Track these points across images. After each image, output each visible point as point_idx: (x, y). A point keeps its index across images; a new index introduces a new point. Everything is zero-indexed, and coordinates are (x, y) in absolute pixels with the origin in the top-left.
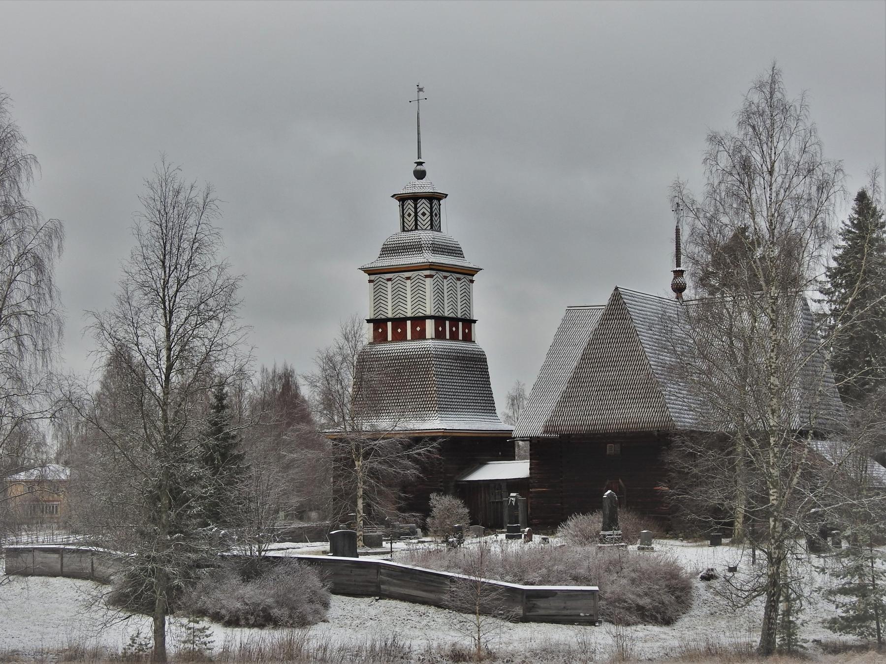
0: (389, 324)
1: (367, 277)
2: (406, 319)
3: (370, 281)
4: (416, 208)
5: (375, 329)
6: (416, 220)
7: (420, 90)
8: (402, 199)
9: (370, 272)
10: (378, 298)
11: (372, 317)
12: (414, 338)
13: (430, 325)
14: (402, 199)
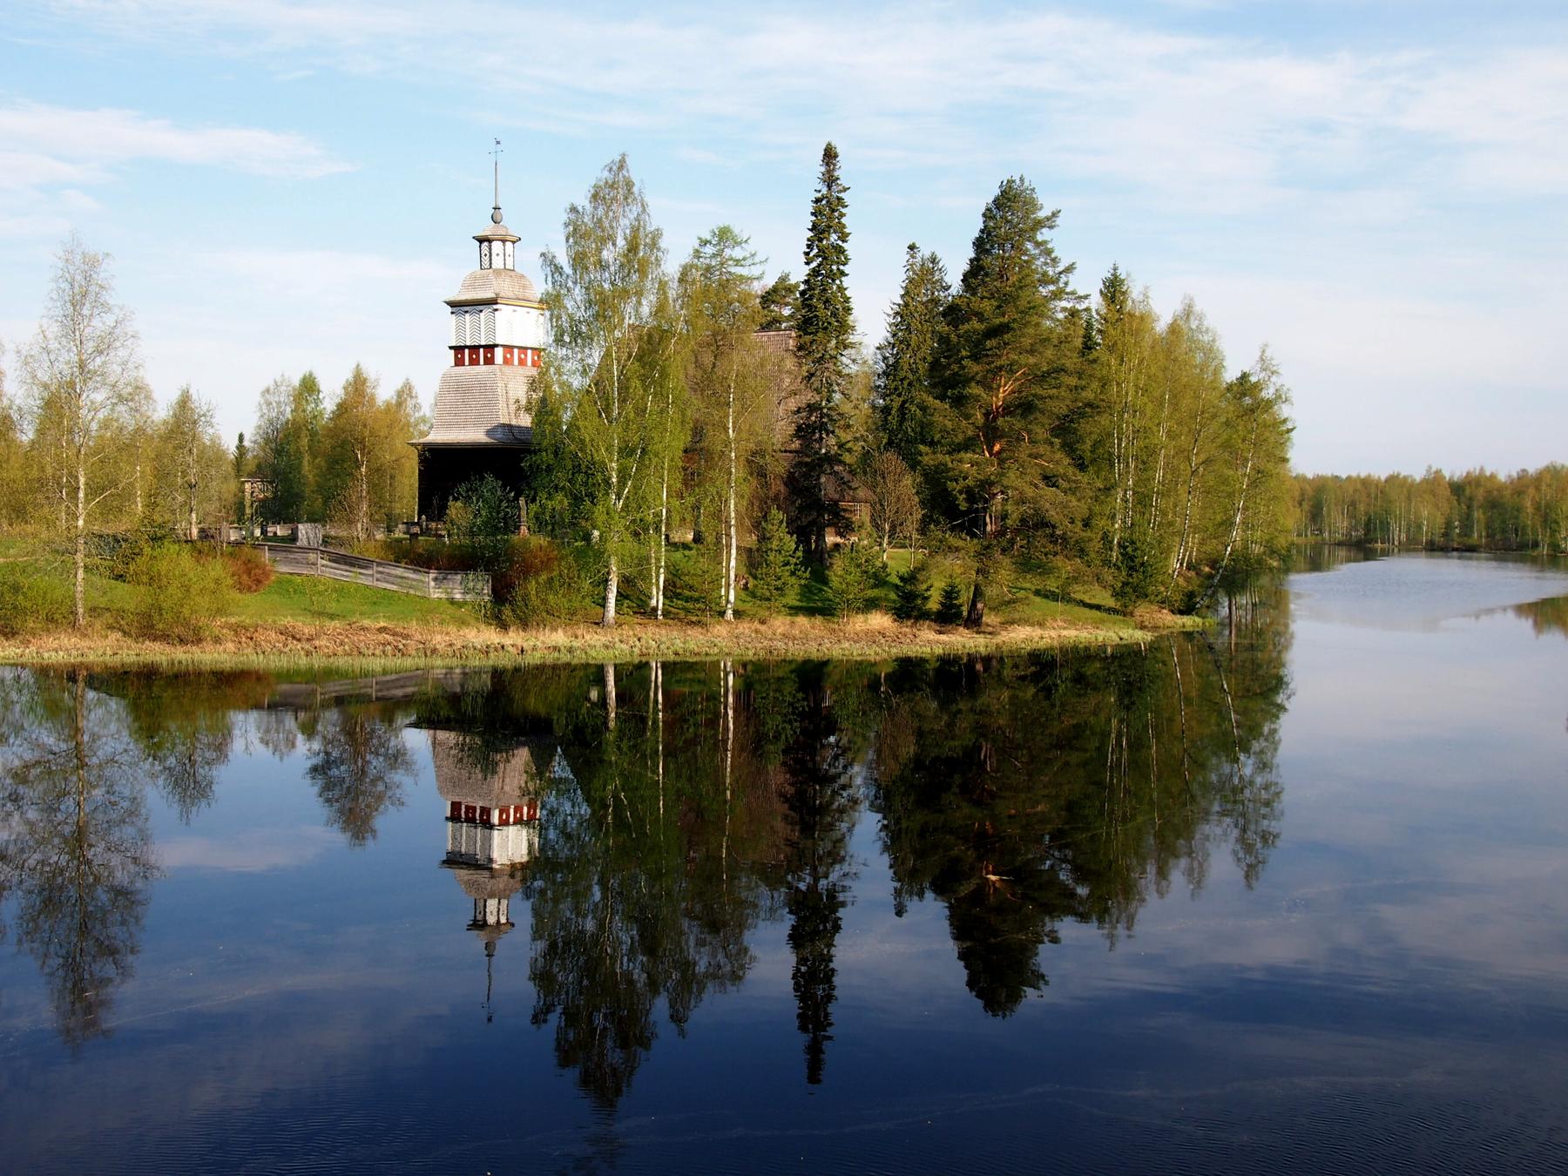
0: (467, 351)
1: (449, 309)
2: (480, 346)
3: (452, 313)
4: (490, 249)
5: (456, 356)
6: (491, 260)
7: (498, 143)
8: (481, 240)
9: (452, 304)
10: (460, 329)
11: (454, 344)
12: (486, 363)
13: (499, 352)
14: (481, 240)
